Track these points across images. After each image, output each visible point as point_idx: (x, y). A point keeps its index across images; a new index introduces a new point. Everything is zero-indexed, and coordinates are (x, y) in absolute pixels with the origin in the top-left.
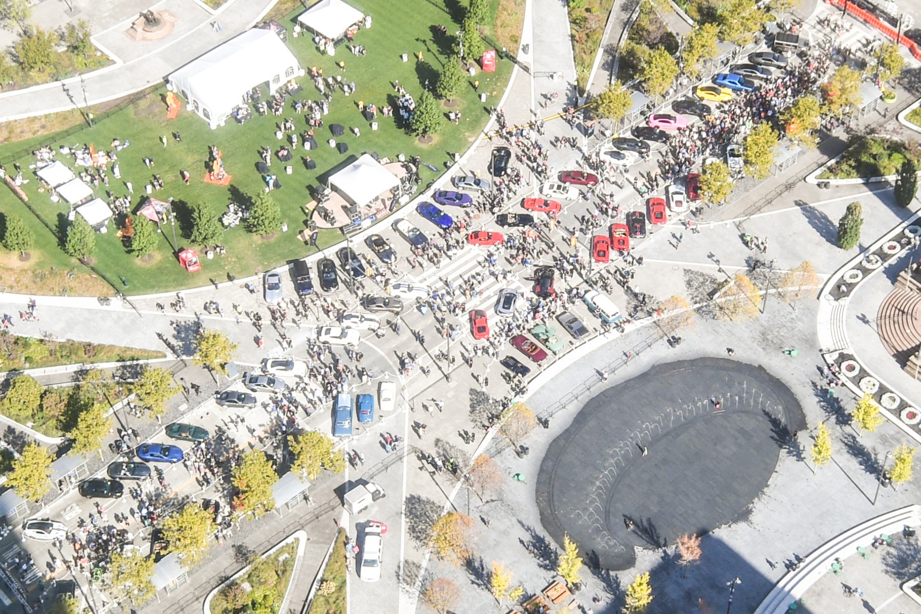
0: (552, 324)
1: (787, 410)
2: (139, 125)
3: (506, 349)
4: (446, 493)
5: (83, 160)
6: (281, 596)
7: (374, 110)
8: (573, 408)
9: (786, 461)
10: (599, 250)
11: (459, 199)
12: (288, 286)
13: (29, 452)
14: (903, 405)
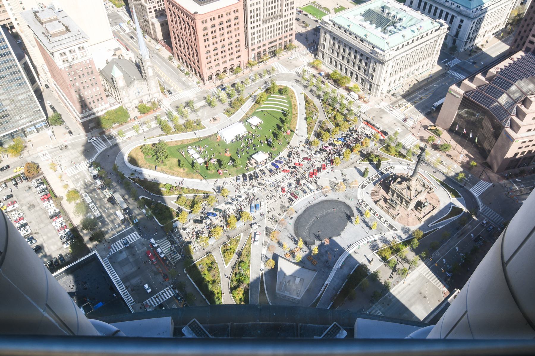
0: (299, 191)
1: (350, 212)
2: (210, 143)
3: (289, 195)
4: (274, 226)
5: (198, 149)
6: (237, 247)
7: (263, 141)
8: (303, 209)
9: (349, 223)
10: (311, 175)
11: (281, 162)
12: (242, 179)
13: (183, 213)
14: (375, 212)
